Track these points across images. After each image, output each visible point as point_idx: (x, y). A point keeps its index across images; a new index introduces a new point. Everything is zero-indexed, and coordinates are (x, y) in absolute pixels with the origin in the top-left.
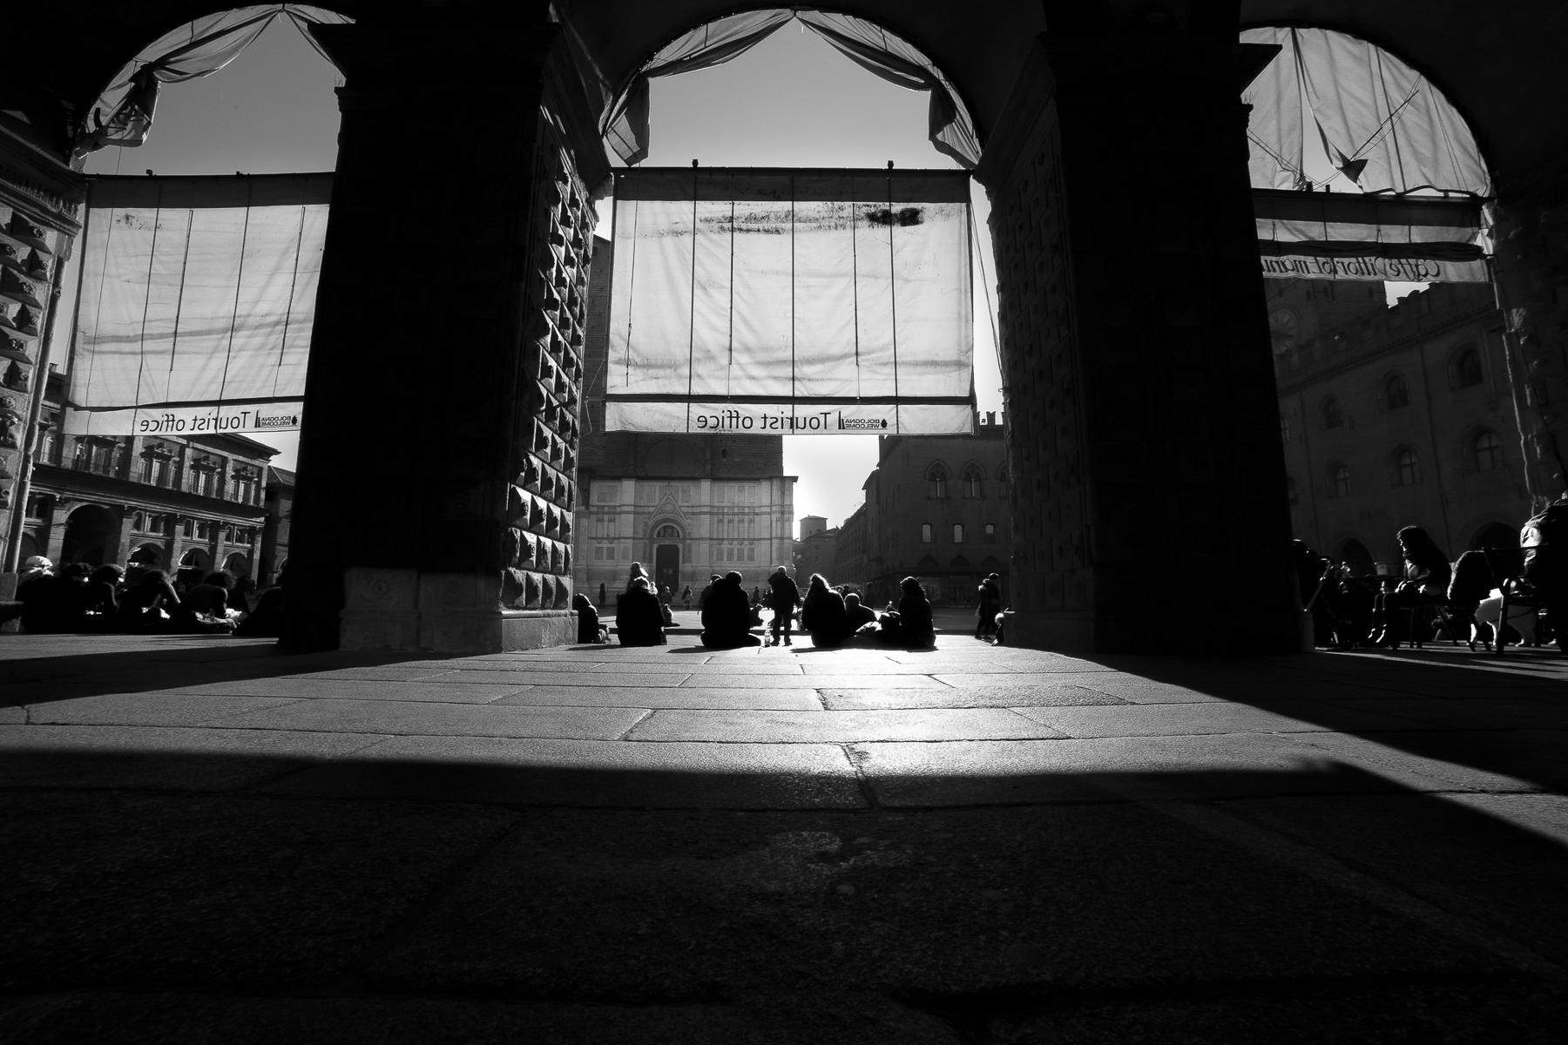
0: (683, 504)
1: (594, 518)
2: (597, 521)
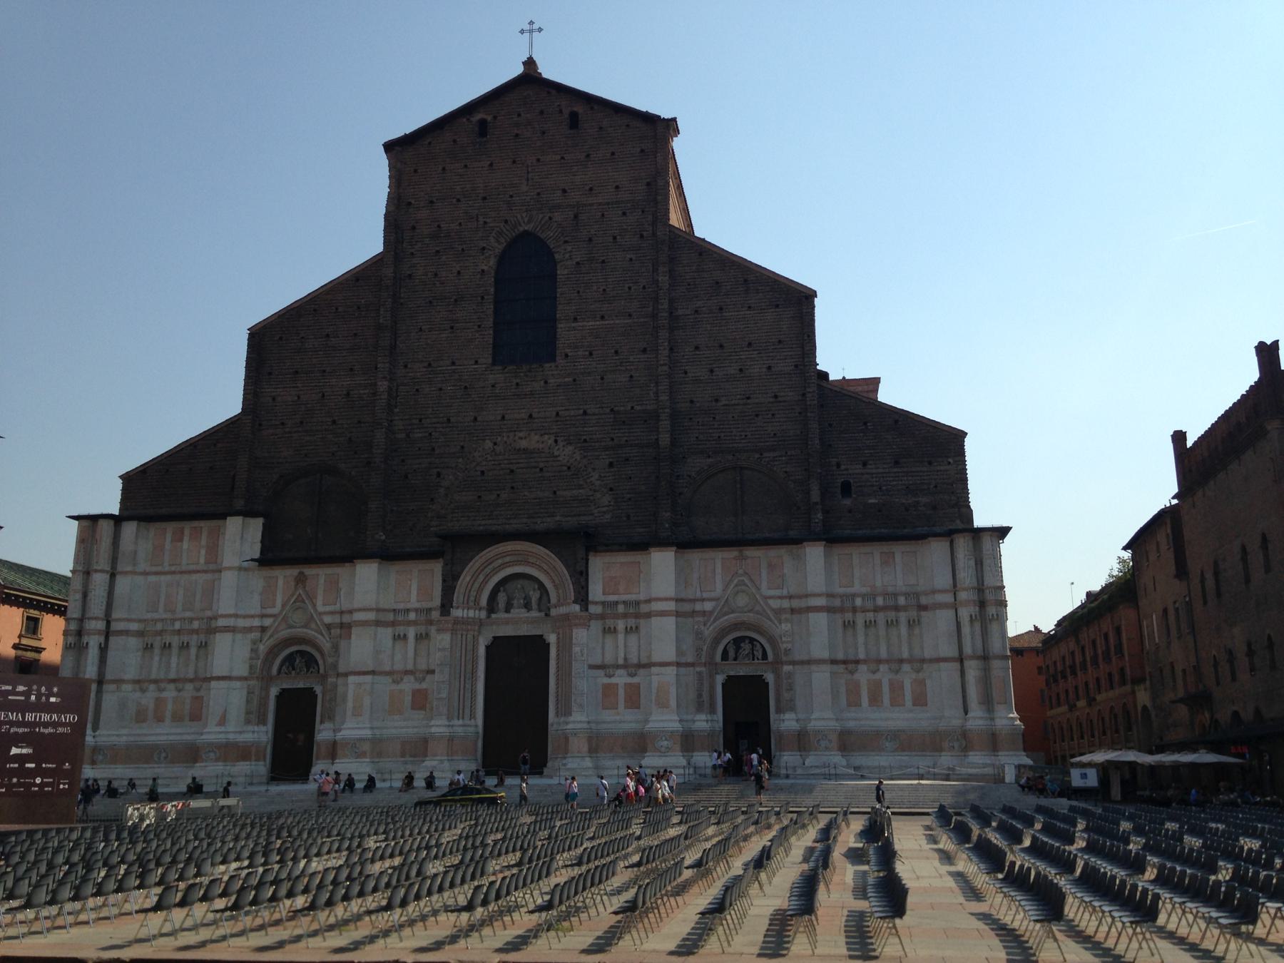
0: (772, 593)
1: (596, 626)
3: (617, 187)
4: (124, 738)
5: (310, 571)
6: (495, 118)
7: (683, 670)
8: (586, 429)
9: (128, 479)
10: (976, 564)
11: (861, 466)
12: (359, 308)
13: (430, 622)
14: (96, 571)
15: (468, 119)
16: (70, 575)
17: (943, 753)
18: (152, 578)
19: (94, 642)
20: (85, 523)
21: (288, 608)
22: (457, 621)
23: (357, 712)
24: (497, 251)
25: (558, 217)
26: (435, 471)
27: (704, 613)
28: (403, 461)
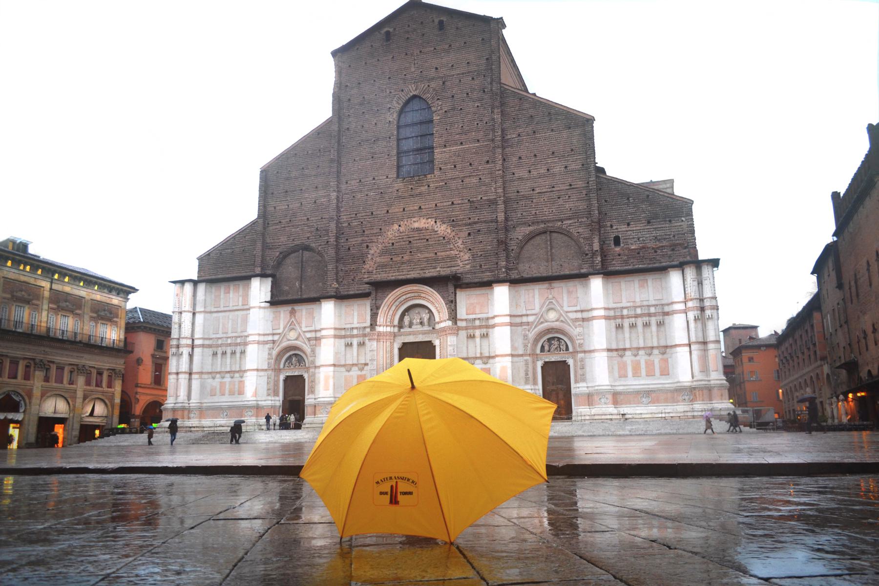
1: (463, 334)
2: (468, 337)
3: (468, 63)
4: (205, 405)
5: (297, 307)
6: (395, 29)
7: (516, 359)
8: (453, 213)
9: (201, 259)
10: (698, 284)
11: (626, 226)
12: (320, 150)
13: (365, 335)
14: (185, 311)
16: (171, 314)
17: (679, 404)
18: (215, 315)
19: (185, 351)
20: (178, 285)
21: (287, 329)
22: (379, 334)
23: (327, 389)
24: (397, 108)
25: (433, 85)
26: (365, 244)
27: (528, 323)
28: (347, 240)
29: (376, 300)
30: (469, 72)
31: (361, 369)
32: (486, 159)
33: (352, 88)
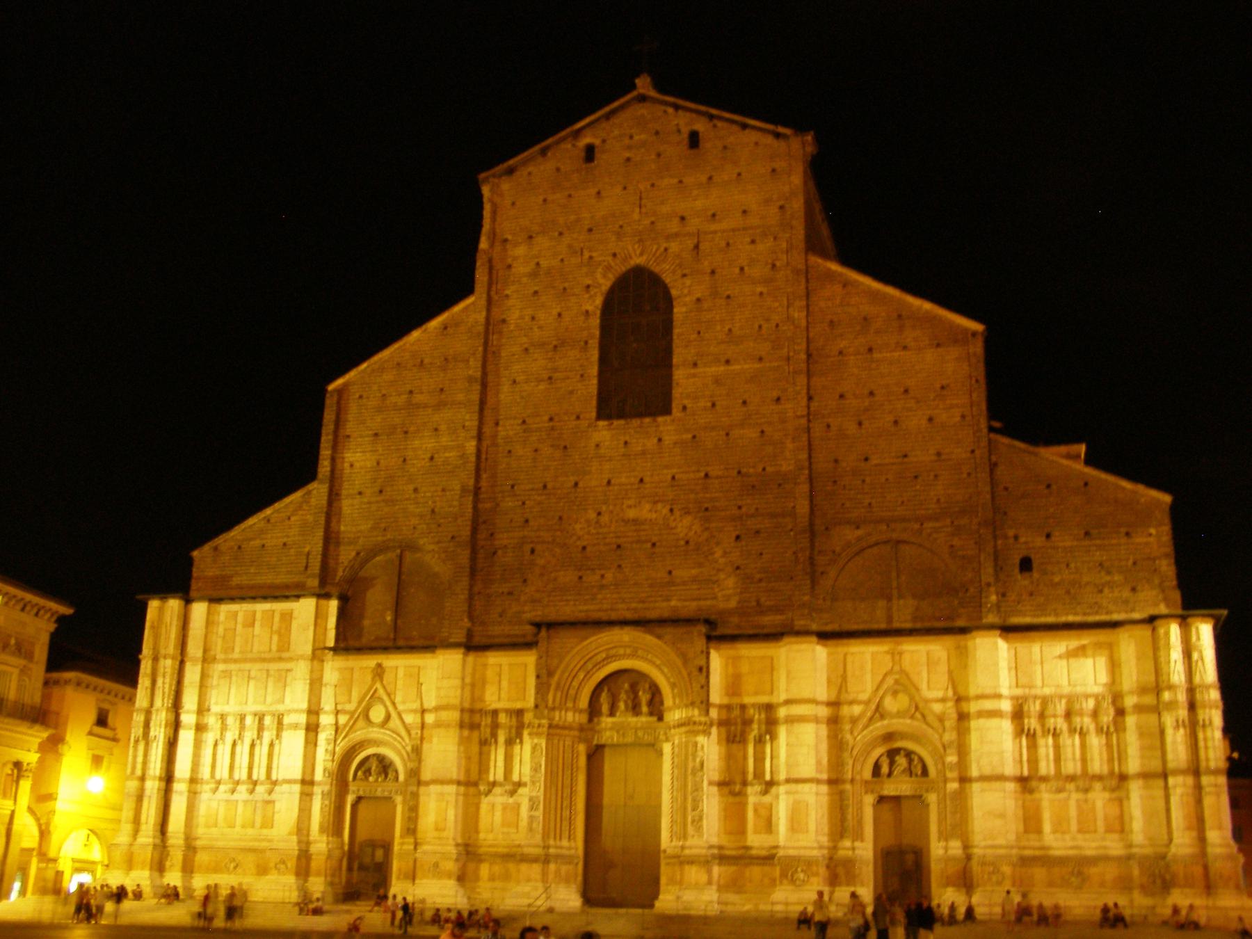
3: (744, 212)
6: (604, 141)
8: (708, 495)
11: (1044, 538)
15: (574, 145)
25: (674, 247)
29: (548, 656)
30: (745, 229)
31: (512, 793)
32: (775, 394)
33: (516, 245)
